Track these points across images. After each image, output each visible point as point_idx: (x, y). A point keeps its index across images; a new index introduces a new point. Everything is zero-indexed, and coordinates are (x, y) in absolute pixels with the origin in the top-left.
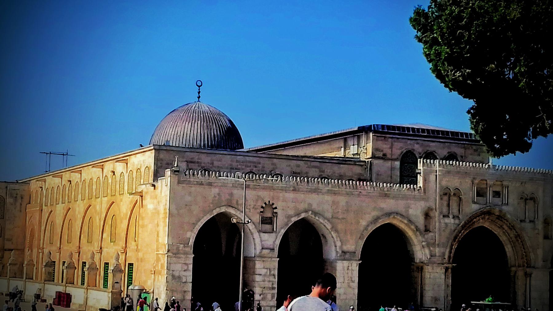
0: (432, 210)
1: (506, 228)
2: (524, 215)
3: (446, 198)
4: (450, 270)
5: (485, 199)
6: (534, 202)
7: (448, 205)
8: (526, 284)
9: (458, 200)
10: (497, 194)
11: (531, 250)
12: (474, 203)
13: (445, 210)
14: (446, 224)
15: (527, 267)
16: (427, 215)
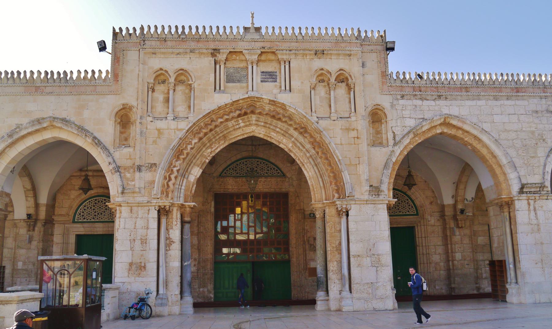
0: (131, 108)
1: (296, 134)
2: (328, 109)
3: (161, 88)
4: (176, 215)
5: (244, 85)
6: (347, 85)
7: (167, 100)
8: (340, 231)
9: (187, 91)
10: (270, 76)
11: (342, 167)
12: (217, 88)
13: (160, 108)
14: (160, 132)
15: (339, 198)
16: (124, 119)
